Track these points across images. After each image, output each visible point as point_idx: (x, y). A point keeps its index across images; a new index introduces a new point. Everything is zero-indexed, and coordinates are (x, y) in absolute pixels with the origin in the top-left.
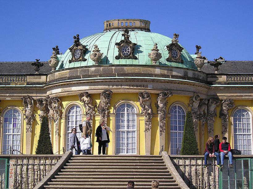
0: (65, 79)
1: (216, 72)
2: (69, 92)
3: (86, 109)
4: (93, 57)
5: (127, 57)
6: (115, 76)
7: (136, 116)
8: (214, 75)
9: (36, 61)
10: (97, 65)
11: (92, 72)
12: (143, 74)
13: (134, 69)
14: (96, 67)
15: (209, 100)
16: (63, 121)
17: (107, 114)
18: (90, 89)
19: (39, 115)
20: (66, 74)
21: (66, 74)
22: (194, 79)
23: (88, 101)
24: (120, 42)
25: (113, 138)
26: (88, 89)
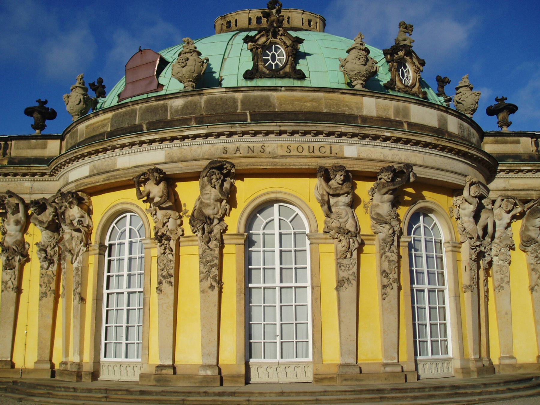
0: (101, 137)
1: (505, 130)
2: (108, 174)
3: (156, 222)
4: (179, 70)
5: (276, 73)
6: (243, 118)
7: (308, 242)
8: (499, 138)
9: (37, 104)
10: (190, 89)
11: (177, 111)
12: (326, 114)
13: (299, 100)
14: (187, 96)
15: (493, 202)
16: (93, 259)
17: (218, 236)
18: (167, 161)
19: (37, 244)
20: (104, 126)
21: (104, 126)
22: (463, 140)
23: (161, 197)
24: (256, 35)
25: (238, 310)
26: (163, 161)
